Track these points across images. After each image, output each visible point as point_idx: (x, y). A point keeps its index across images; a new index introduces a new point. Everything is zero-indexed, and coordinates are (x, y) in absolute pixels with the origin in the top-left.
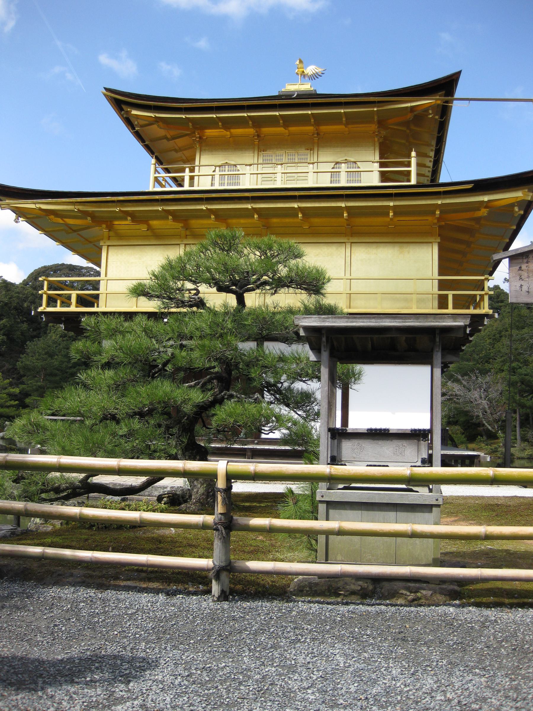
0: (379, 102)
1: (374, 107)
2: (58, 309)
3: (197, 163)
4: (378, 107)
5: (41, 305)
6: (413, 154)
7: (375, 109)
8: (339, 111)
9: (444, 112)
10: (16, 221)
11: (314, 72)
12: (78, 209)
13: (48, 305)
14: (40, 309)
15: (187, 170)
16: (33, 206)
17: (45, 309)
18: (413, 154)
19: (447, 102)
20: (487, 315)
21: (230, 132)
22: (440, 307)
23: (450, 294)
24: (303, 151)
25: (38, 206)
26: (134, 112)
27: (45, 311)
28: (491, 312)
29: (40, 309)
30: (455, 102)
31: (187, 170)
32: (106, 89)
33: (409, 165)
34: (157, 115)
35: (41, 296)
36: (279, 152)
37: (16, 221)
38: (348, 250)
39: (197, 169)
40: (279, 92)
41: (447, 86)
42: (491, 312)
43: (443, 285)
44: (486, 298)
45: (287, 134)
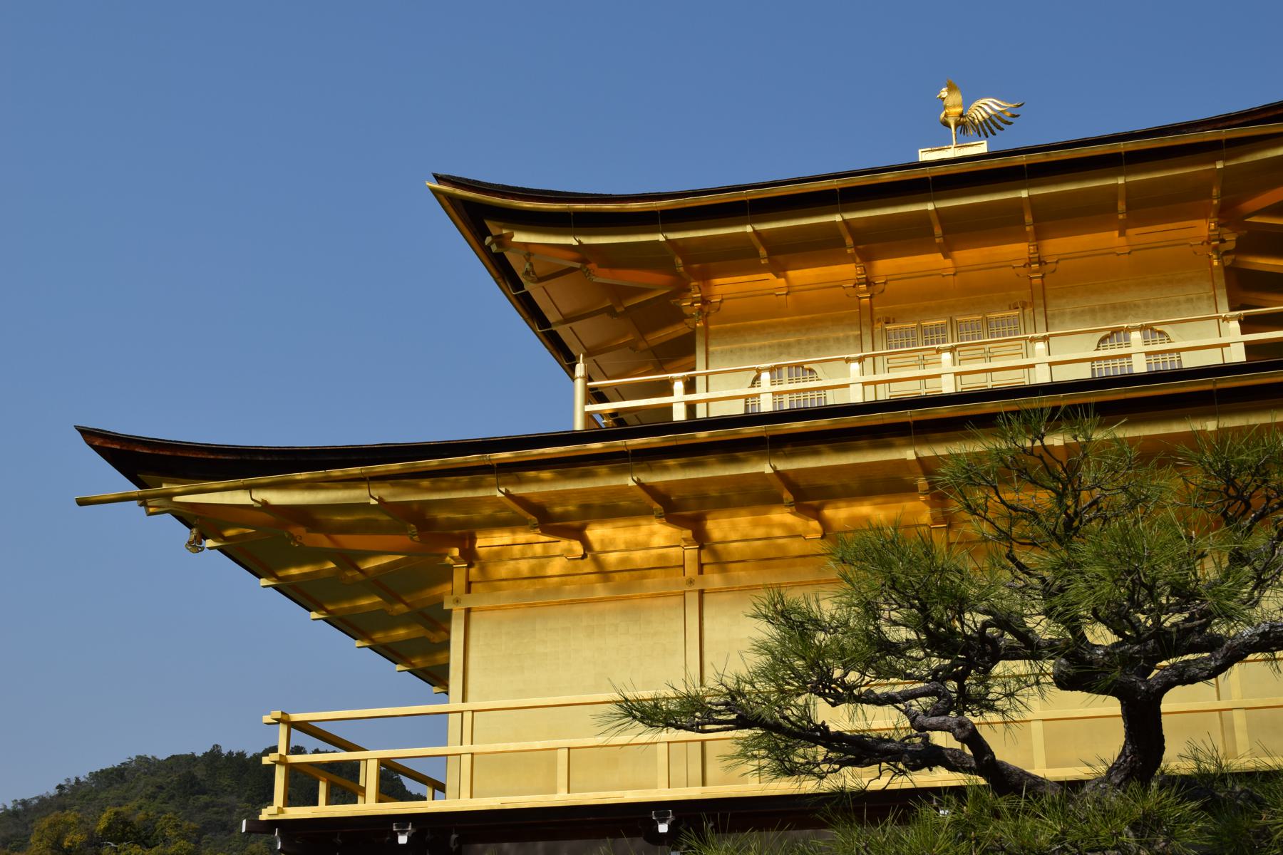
0: (1231, 143)
1: (1213, 162)
2: (323, 810)
3: (700, 369)
4: (1225, 159)
5: (269, 800)
7: (1219, 165)
10: (195, 545)
12: (380, 500)
13: (290, 801)
14: (266, 814)
15: (679, 387)
16: (241, 498)
17: (280, 811)
25: (260, 495)
26: (520, 237)
27: (281, 817)
31: (679, 387)
32: (439, 179)
34: (586, 240)
35: (270, 769)
37: (195, 545)
39: (700, 383)
45: (952, 271)
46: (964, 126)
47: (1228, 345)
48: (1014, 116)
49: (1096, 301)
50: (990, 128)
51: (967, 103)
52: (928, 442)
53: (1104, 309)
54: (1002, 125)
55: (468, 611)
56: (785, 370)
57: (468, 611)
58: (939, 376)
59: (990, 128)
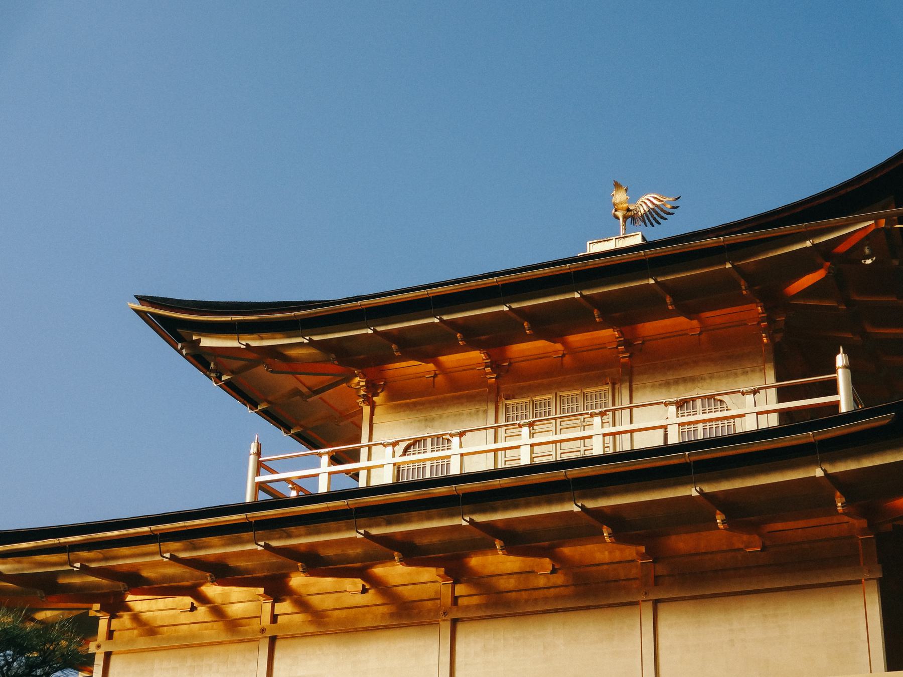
6: (841, 360)
8: (645, 282)
11: (651, 206)
18: (841, 360)
21: (438, 364)
26: (207, 342)
32: (142, 299)
33: (831, 388)
46: (631, 217)
47: (743, 416)
48: (674, 208)
49: (671, 376)
50: (654, 219)
51: (633, 199)
52: (833, 460)
53: (677, 382)
54: (665, 216)
55: (108, 655)
56: (429, 441)
57: (108, 655)
58: (518, 447)
59: (654, 219)
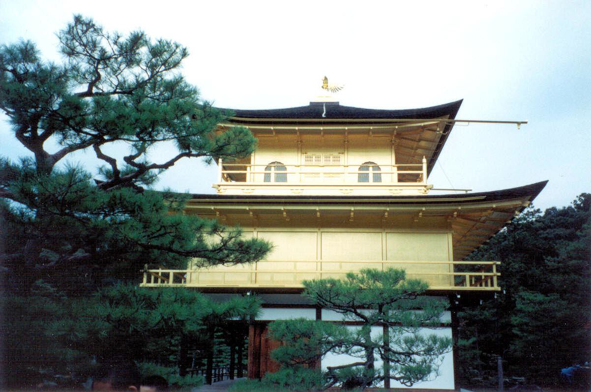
0: (400, 122)
4: (398, 125)
5: (142, 282)
9: (448, 128)
19: (451, 123)
20: (497, 292)
22: (456, 284)
23: (467, 274)
24: (336, 154)
28: (499, 289)
29: (141, 285)
30: (456, 123)
33: (421, 169)
36: (318, 154)
38: (384, 239)
40: (311, 103)
41: (449, 111)
42: (499, 289)
43: (458, 268)
44: (495, 279)
48: (342, 88)
